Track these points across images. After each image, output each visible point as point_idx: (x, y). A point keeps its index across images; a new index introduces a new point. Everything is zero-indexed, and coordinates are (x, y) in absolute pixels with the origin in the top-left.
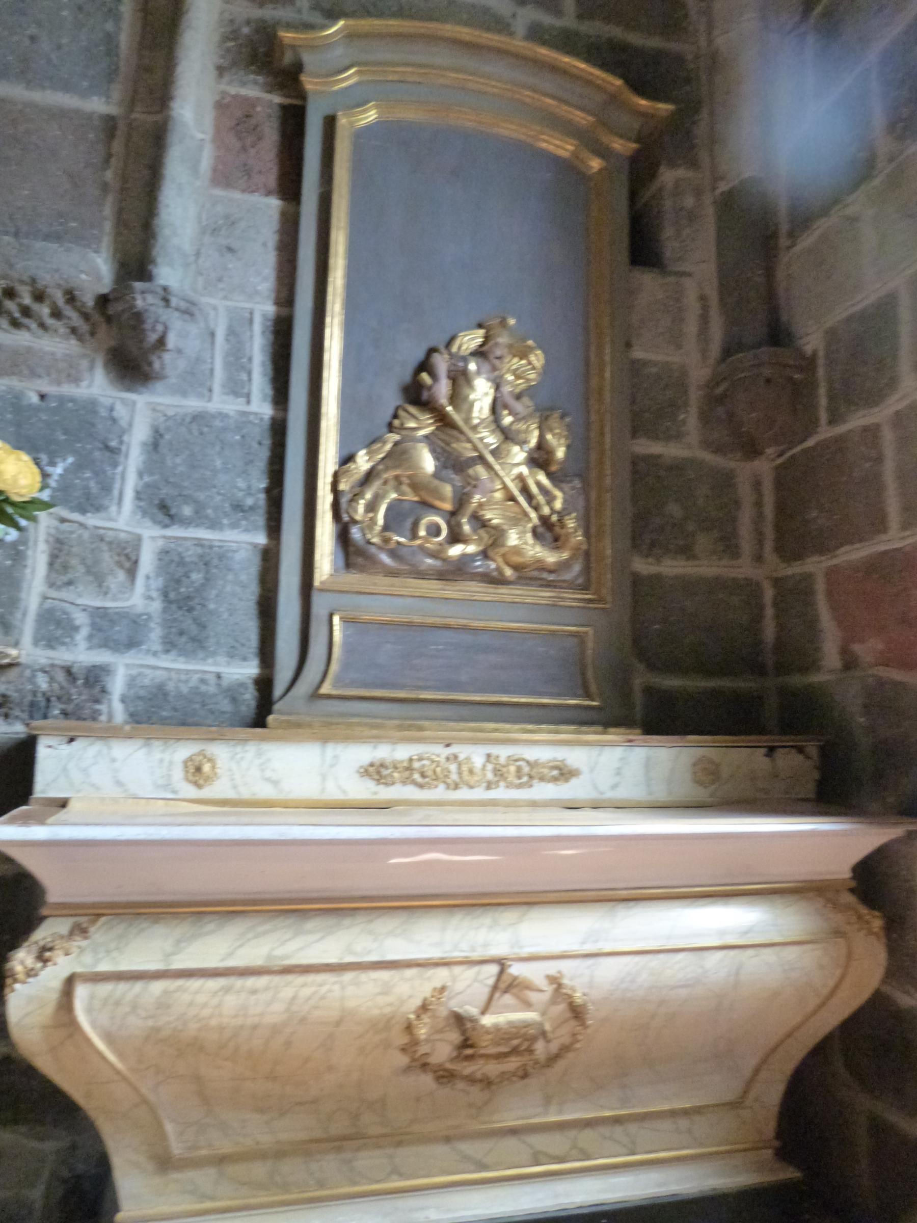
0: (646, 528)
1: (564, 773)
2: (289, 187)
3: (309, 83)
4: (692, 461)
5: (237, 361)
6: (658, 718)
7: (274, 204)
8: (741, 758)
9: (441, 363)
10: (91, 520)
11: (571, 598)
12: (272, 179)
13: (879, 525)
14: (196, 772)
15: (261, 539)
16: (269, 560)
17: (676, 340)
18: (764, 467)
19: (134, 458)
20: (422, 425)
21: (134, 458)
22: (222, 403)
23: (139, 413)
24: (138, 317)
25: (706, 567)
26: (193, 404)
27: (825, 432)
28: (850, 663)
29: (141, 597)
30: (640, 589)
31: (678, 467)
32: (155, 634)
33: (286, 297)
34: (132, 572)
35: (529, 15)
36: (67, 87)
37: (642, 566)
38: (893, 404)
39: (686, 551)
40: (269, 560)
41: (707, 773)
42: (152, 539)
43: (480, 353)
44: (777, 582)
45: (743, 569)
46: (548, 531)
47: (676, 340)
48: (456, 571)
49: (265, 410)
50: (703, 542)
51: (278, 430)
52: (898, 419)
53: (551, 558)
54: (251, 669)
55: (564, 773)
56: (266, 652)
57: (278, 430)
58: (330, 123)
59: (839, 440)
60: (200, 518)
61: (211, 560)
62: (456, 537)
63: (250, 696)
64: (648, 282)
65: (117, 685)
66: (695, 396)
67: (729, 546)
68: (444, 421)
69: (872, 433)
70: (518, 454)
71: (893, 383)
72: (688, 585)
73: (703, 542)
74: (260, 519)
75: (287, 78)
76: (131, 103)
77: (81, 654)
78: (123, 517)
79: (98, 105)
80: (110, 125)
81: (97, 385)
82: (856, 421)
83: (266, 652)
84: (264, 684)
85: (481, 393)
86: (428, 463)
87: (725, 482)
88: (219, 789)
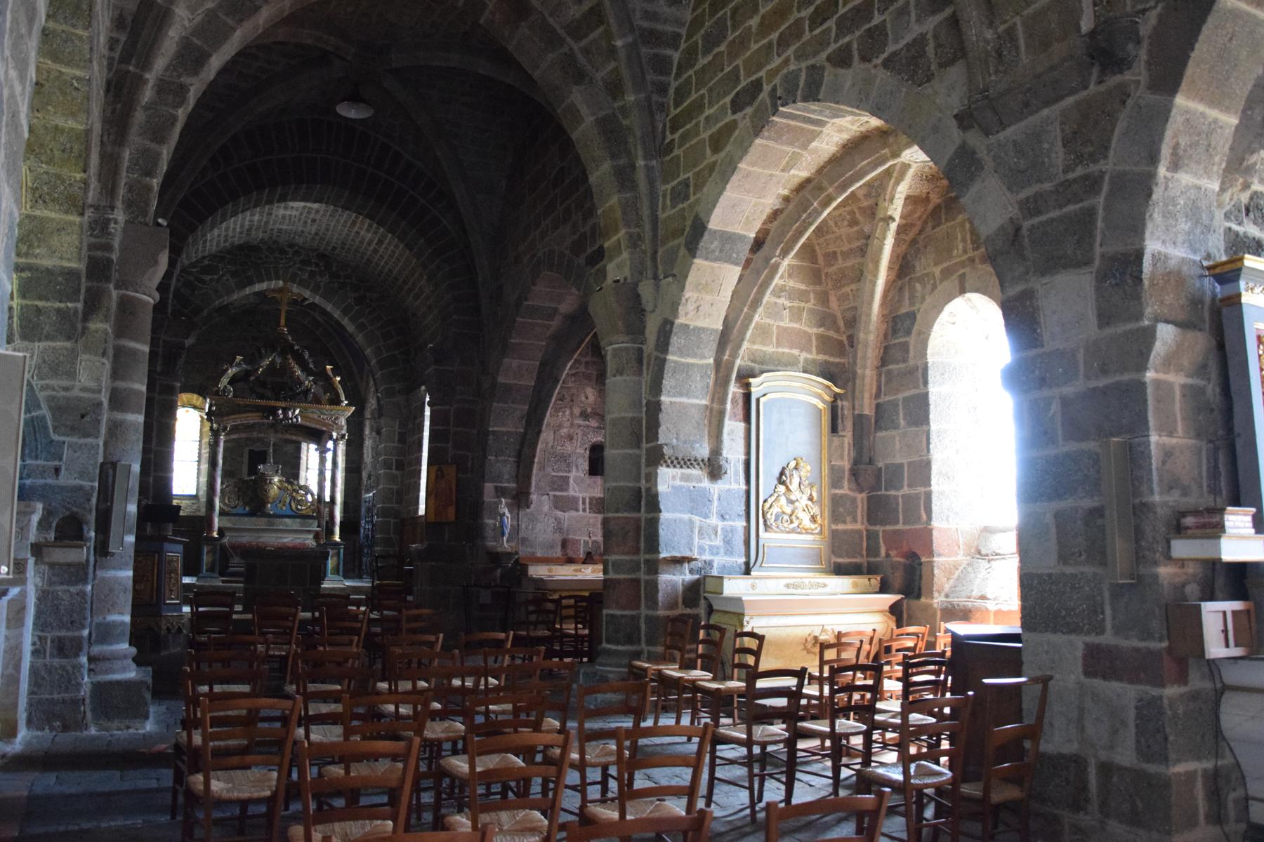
0: (836, 517)
1: (825, 585)
2: (747, 419)
3: (753, 389)
4: (846, 495)
5: (736, 474)
6: (839, 570)
7: (742, 425)
8: (862, 580)
9: (787, 472)
10: (708, 521)
11: (818, 537)
12: (741, 417)
13: (897, 522)
14: (753, 587)
15: (744, 524)
16: (748, 529)
17: (842, 457)
18: (864, 495)
19: (716, 503)
20: (782, 489)
21: (716, 503)
22: (734, 486)
23: (716, 488)
24: (720, 467)
25: (849, 527)
26: (727, 487)
27: (883, 492)
28: (888, 555)
29: (718, 542)
30: (834, 534)
31: (842, 496)
32: (722, 551)
33: (748, 453)
34: (716, 534)
35: (804, 355)
36: (697, 398)
37: (834, 527)
38: (901, 493)
39: (844, 522)
40: (748, 529)
41: (855, 585)
42: (721, 524)
43: (796, 468)
44: (867, 531)
45: (858, 526)
46: (813, 519)
47: (842, 457)
48: (793, 531)
49: (744, 487)
50: (849, 519)
51: (748, 493)
52: (903, 496)
53: (813, 526)
54: (743, 560)
55: (825, 585)
56: (748, 555)
57: (748, 493)
58: (758, 400)
59: (888, 496)
60: (731, 519)
61: (733, 530)
62: (792, 522)
63: (743, 567)
64: (836, 440)
65: (715, 565)
66: (847, 473)
67: (855, 520)
68: (788, 489)
69: (896, 497)
70: (805, 497)
71: (902, 487)
72: (845, 532)
73: (849, 519)
74: (744, 518)
75: (748, 385)
76: (712, 400)
77: (707, 557)
78: (714, 520)
79: (704, 402)
80: (706, 406)
81: (706, 483)
82: (892, 493)
83: (748, 555)
84: (747, 564)
85: (796, 481)
86: (783, 500)
87: (854, 500)
88: (757, 591)
